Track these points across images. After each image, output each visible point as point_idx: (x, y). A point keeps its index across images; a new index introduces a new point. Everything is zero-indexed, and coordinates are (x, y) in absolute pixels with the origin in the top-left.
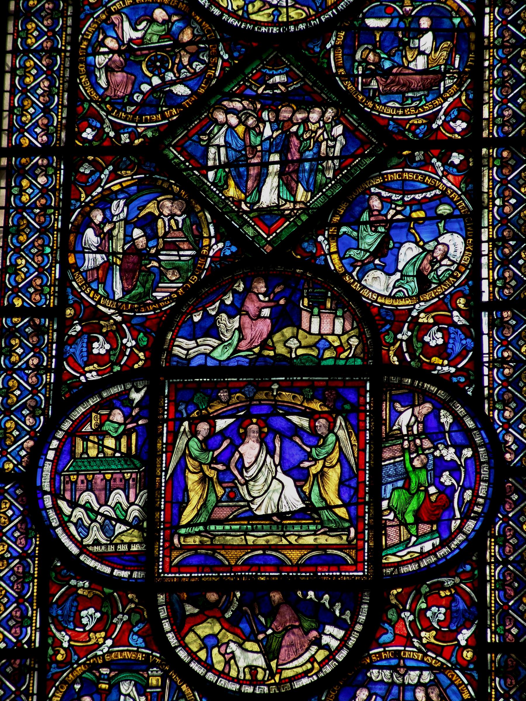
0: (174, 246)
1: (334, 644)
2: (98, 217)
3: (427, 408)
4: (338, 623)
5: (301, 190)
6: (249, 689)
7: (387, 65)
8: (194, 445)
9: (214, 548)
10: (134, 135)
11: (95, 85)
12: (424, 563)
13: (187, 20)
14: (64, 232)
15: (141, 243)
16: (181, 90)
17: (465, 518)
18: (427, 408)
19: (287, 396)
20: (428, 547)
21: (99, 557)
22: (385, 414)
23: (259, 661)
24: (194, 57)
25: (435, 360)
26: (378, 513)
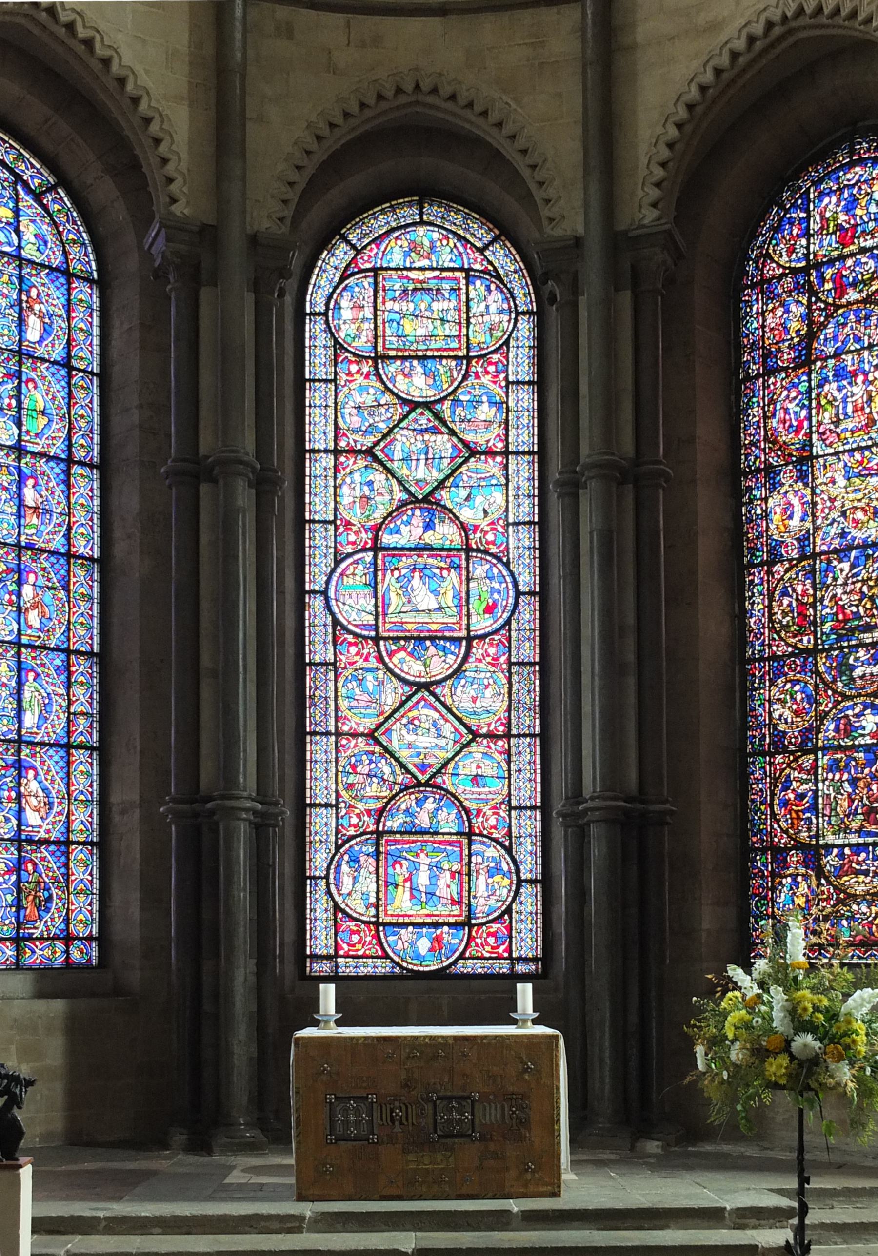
0: (381, 494)
1: (451, 662)
2: (348, 480)
3: (488, 566)
4: (452, 653)
5: (434, 470)
6: (418, 679)
7: (469, 417)
8: (393, 580)
9: (402, 623)
10: (362, 445)
11: (345, 422)
12: (487, 630)
13: (383, 392)
14: (335, 487)
15: (367, 493)
16: (382, 426)
17: (503, 612)
18: (488, 566)
19: (430, 561)
20: (488, 624)
21: (356, 626)
22: (471, 569)
23: (422, 668)
24: (387, 410)
25: (491, 546)
26: (468, 609)
